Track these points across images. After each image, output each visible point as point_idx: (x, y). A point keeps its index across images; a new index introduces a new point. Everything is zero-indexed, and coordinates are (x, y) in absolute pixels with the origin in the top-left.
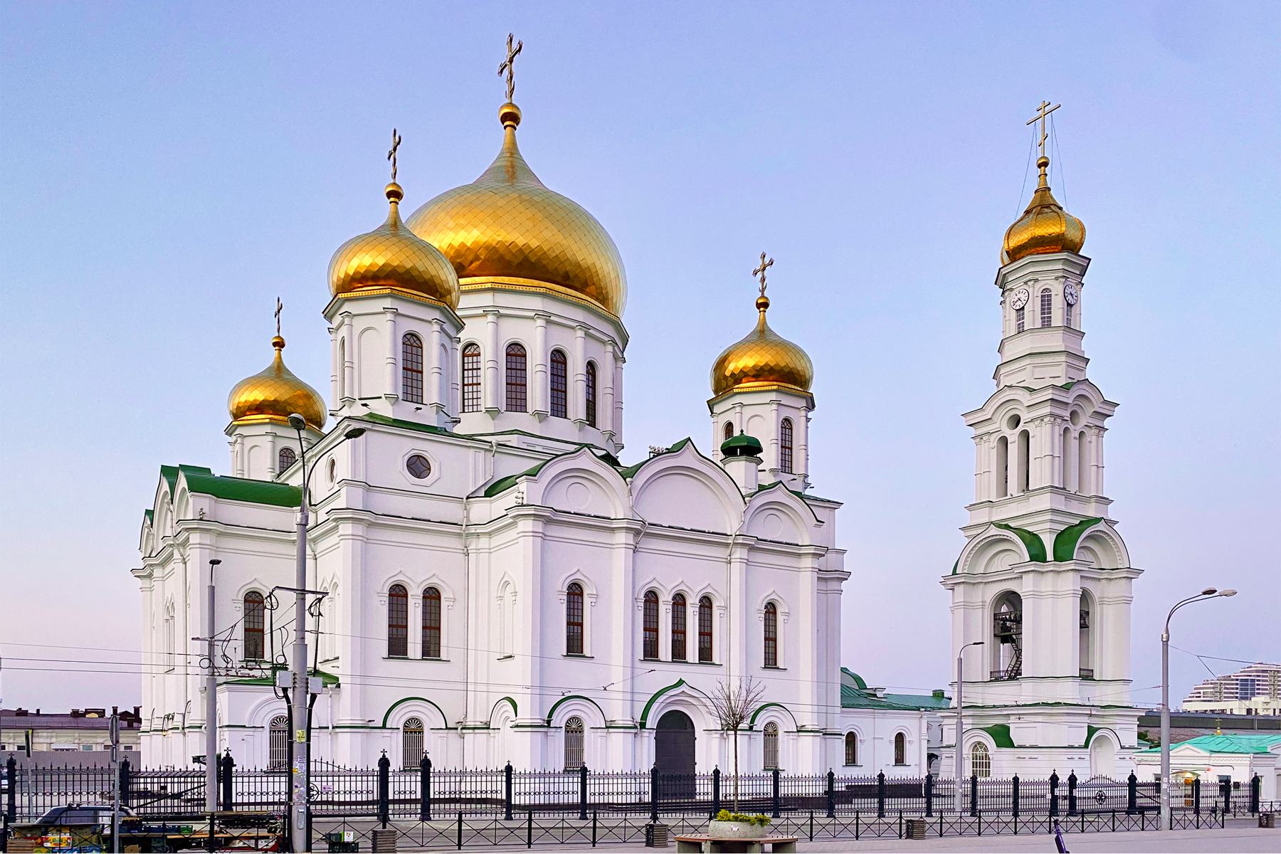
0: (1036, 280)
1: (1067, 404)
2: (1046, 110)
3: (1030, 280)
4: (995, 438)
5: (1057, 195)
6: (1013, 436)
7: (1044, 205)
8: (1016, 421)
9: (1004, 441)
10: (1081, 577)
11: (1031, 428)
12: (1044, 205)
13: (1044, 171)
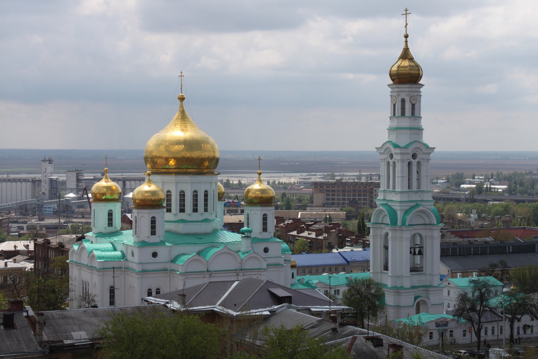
7: (406, 55)
9: (388, 163)
12: (406, 55)
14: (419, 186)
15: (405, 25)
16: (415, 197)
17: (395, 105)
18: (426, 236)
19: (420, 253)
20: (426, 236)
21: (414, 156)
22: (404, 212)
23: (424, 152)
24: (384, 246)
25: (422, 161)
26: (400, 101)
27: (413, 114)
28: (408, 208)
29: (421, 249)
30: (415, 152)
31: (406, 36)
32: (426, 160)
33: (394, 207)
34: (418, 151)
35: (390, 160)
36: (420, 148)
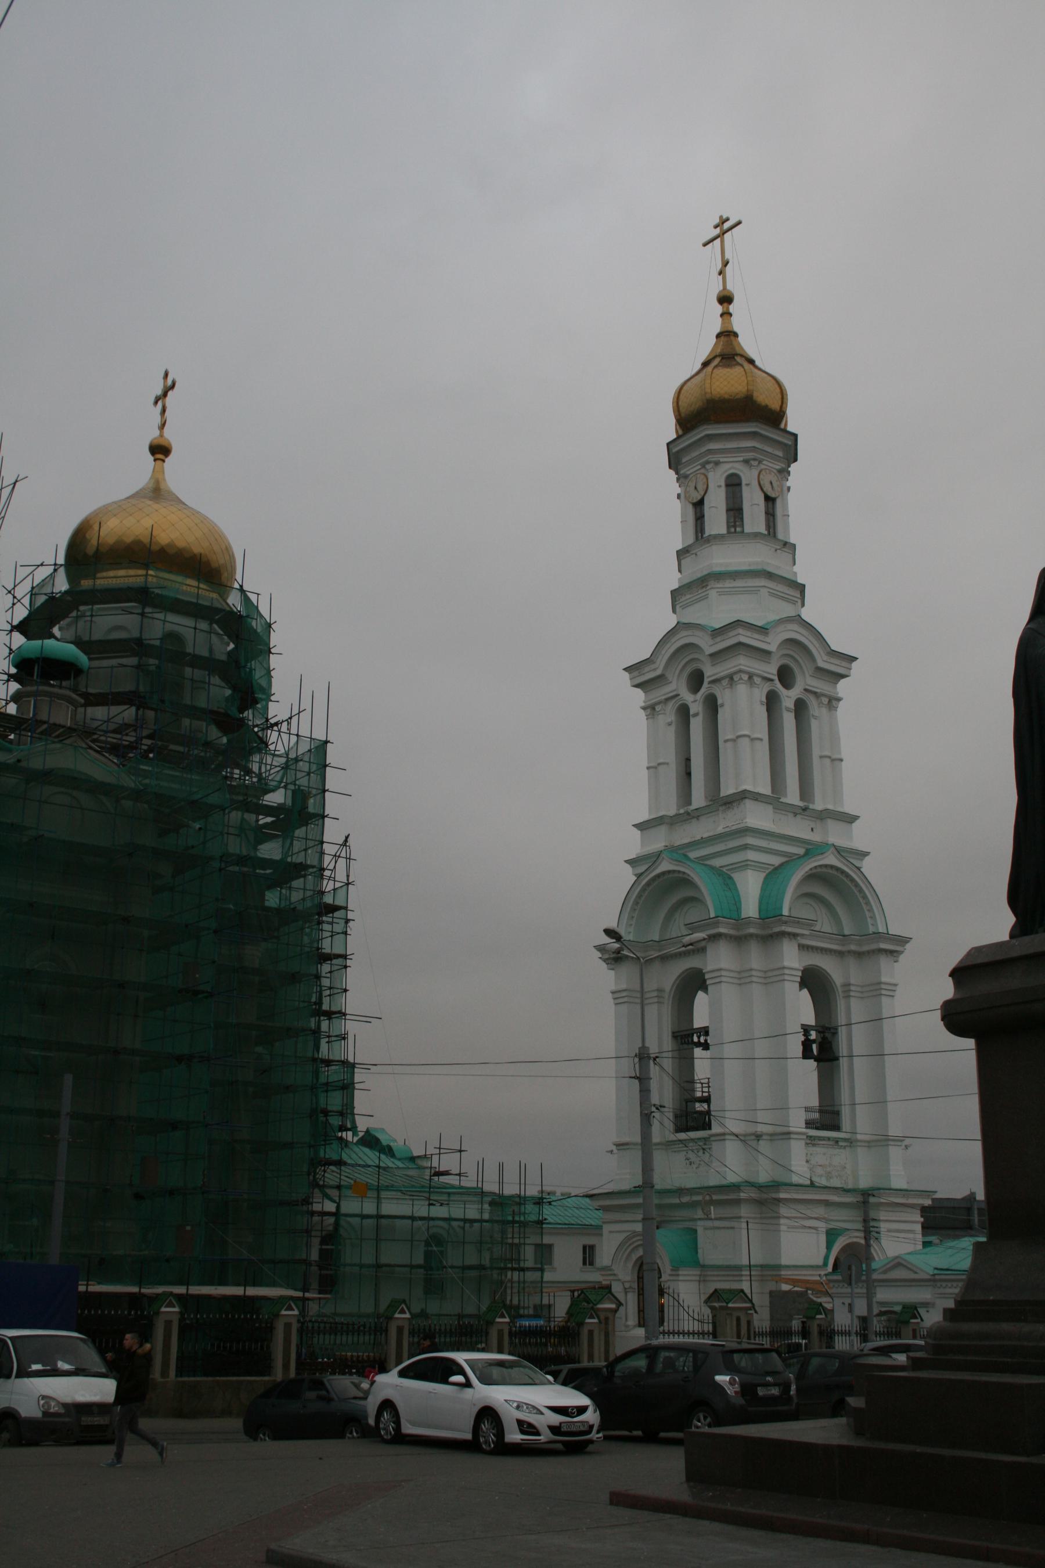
0: (717, 463)
1: (768, 653)
2: (724, 227)
4: (671, 708)
5: (747, 343)
6: (695, 703)
8: (696, 680)
10: (799, 945)
11: (717, 690)
13: (728, 308)
14: (806, 790)
15: (719, 266)
16: (799, 829)
17: (699, 505)
18: (847, 985)
20: (847, 985)
21: (785, 676)
22: (762, 875)
23: (821, 664)
24: (675, 1036)
25: (812, 702)
26: (723, 484)
28: (776, 861)
31: (725, 299)
32: (825, 700)
33: (717, 862)
34: (796, 661)
35: (688, 697)
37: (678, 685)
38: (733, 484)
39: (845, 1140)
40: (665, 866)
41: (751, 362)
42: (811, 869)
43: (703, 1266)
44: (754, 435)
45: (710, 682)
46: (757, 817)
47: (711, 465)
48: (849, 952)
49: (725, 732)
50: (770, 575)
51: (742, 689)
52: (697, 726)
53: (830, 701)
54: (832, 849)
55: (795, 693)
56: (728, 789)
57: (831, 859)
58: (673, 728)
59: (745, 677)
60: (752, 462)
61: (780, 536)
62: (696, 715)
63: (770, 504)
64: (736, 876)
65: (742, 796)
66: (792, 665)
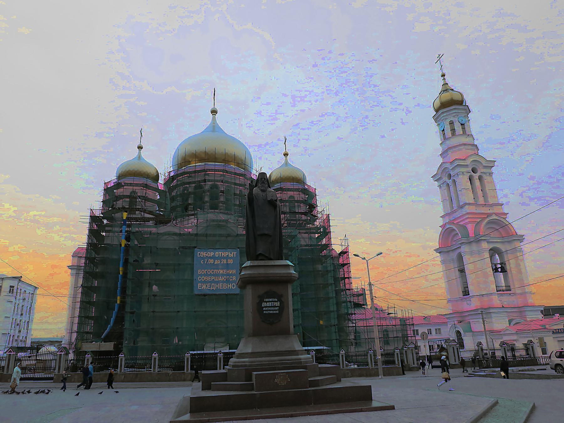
2: (440, 57)
3: (444, 119)
5: (451, 84)
6: (450, 182)
7: (446, 89)
8: (450, 176)
9: (448, 185)
12: (446, 89)
13: (444, 78)
19: (503, 270)
21: (474, 171)
26: (448, 124)
27: (464, 132)
29: (503, 265)
30: (474, 166)
31: (443, 75)
32: (488, 174)
33: (461, 223)
34: (477, 165)
36: (479, 161)
37: (445, 179)
38: (452, 123)
39: (513, 293)
40: (448, 226)
41: (452, 90)
42: (488, 221)
43: (473, 332)
44: (455, 109)
45: (453, 176)
46: (472, 209)
47: (444, 120)
48: (506, 241)
49: (459, 188)
50: (465, 144)
51: (461, 176)
52: (452, 189)
53: (489, 174)
54: (494, 214)
55: (478, 174)
56: (461, 204)
57: (494, 217)
58: (446, 191)
59: (461, 173)
60: (455, 116)
61: (467, 134)
62: (451, 186)
63: (463, 125)
64: (467, 226)
65: (466, 204)
66: (476, 167)
